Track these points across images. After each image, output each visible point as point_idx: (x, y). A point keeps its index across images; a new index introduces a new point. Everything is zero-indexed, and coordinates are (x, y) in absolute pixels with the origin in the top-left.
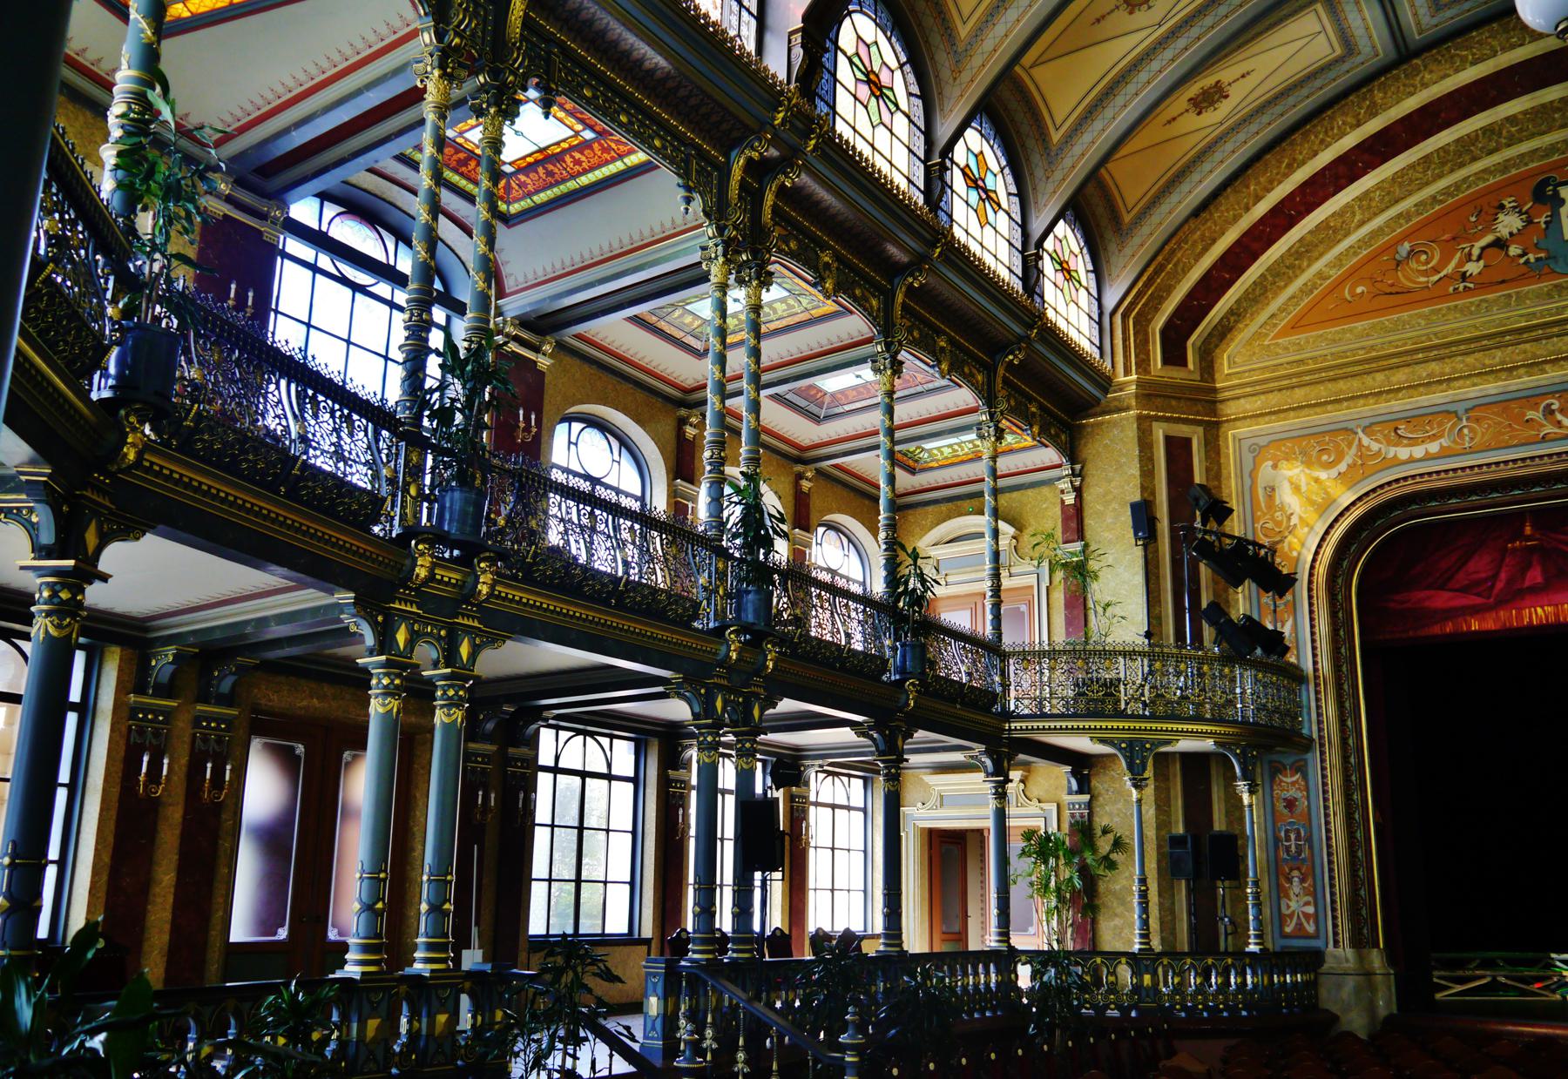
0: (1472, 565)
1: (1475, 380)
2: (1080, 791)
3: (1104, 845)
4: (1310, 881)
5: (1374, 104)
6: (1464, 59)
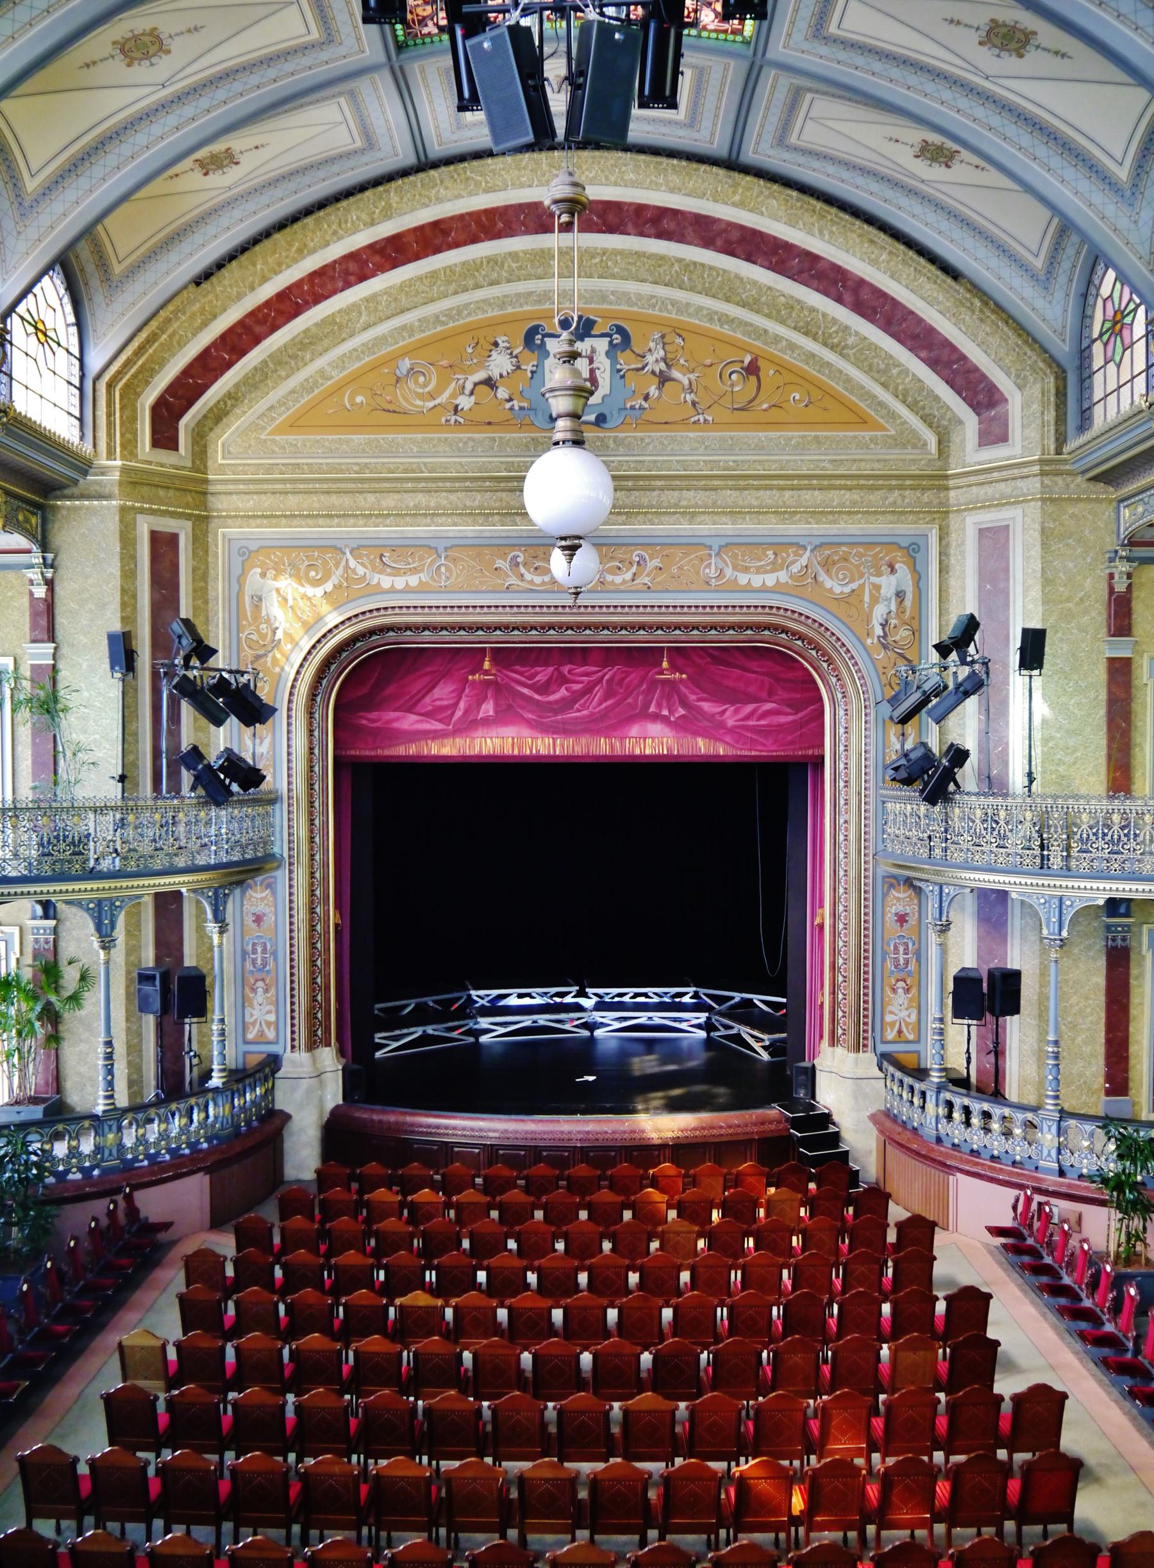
0: (437, 692)
1: (456, 519)
2: (46, 916)
3: (70, 977)
4: (273, 991)
5: (389, 206)
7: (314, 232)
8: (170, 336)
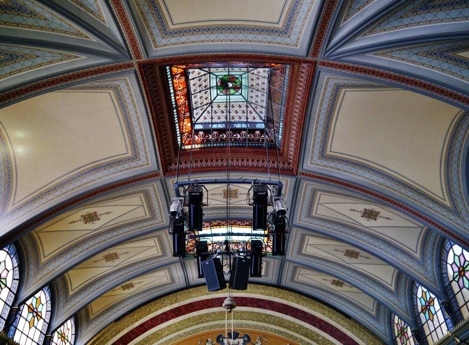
8: (104, 338)
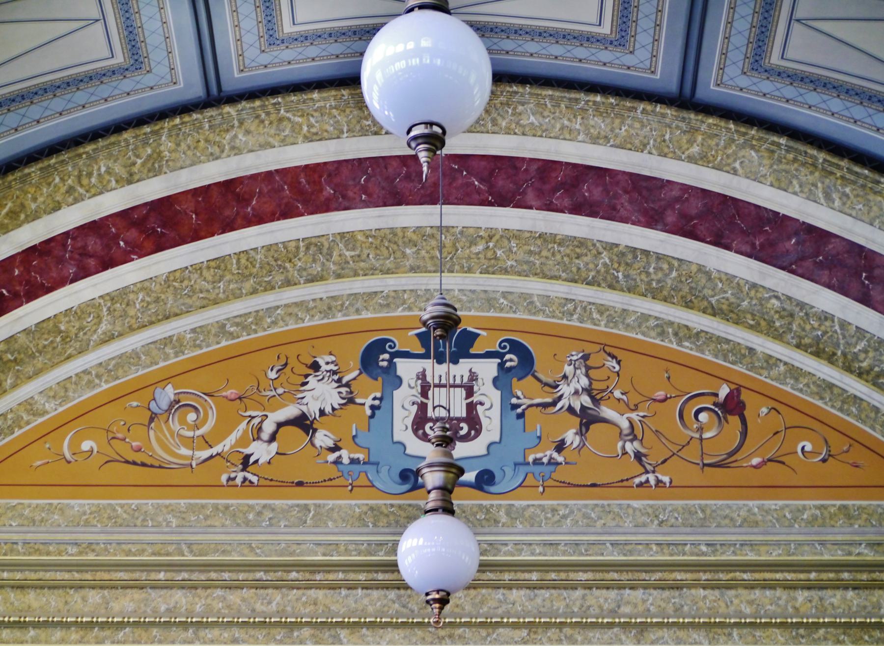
1: (237, 633)
6: (296, 129)
7: (38, 187)
